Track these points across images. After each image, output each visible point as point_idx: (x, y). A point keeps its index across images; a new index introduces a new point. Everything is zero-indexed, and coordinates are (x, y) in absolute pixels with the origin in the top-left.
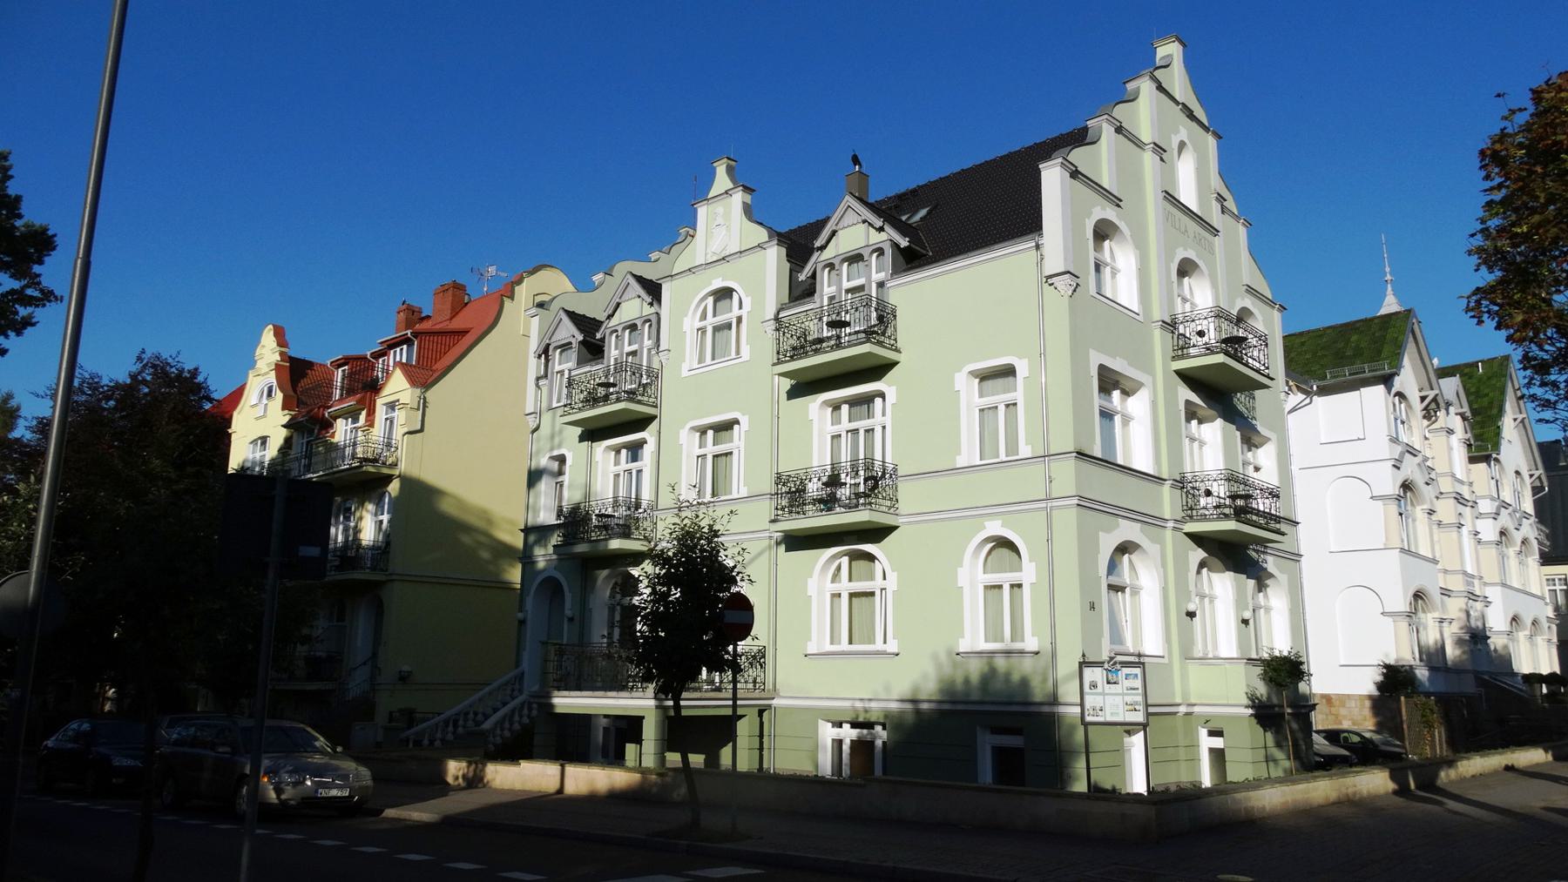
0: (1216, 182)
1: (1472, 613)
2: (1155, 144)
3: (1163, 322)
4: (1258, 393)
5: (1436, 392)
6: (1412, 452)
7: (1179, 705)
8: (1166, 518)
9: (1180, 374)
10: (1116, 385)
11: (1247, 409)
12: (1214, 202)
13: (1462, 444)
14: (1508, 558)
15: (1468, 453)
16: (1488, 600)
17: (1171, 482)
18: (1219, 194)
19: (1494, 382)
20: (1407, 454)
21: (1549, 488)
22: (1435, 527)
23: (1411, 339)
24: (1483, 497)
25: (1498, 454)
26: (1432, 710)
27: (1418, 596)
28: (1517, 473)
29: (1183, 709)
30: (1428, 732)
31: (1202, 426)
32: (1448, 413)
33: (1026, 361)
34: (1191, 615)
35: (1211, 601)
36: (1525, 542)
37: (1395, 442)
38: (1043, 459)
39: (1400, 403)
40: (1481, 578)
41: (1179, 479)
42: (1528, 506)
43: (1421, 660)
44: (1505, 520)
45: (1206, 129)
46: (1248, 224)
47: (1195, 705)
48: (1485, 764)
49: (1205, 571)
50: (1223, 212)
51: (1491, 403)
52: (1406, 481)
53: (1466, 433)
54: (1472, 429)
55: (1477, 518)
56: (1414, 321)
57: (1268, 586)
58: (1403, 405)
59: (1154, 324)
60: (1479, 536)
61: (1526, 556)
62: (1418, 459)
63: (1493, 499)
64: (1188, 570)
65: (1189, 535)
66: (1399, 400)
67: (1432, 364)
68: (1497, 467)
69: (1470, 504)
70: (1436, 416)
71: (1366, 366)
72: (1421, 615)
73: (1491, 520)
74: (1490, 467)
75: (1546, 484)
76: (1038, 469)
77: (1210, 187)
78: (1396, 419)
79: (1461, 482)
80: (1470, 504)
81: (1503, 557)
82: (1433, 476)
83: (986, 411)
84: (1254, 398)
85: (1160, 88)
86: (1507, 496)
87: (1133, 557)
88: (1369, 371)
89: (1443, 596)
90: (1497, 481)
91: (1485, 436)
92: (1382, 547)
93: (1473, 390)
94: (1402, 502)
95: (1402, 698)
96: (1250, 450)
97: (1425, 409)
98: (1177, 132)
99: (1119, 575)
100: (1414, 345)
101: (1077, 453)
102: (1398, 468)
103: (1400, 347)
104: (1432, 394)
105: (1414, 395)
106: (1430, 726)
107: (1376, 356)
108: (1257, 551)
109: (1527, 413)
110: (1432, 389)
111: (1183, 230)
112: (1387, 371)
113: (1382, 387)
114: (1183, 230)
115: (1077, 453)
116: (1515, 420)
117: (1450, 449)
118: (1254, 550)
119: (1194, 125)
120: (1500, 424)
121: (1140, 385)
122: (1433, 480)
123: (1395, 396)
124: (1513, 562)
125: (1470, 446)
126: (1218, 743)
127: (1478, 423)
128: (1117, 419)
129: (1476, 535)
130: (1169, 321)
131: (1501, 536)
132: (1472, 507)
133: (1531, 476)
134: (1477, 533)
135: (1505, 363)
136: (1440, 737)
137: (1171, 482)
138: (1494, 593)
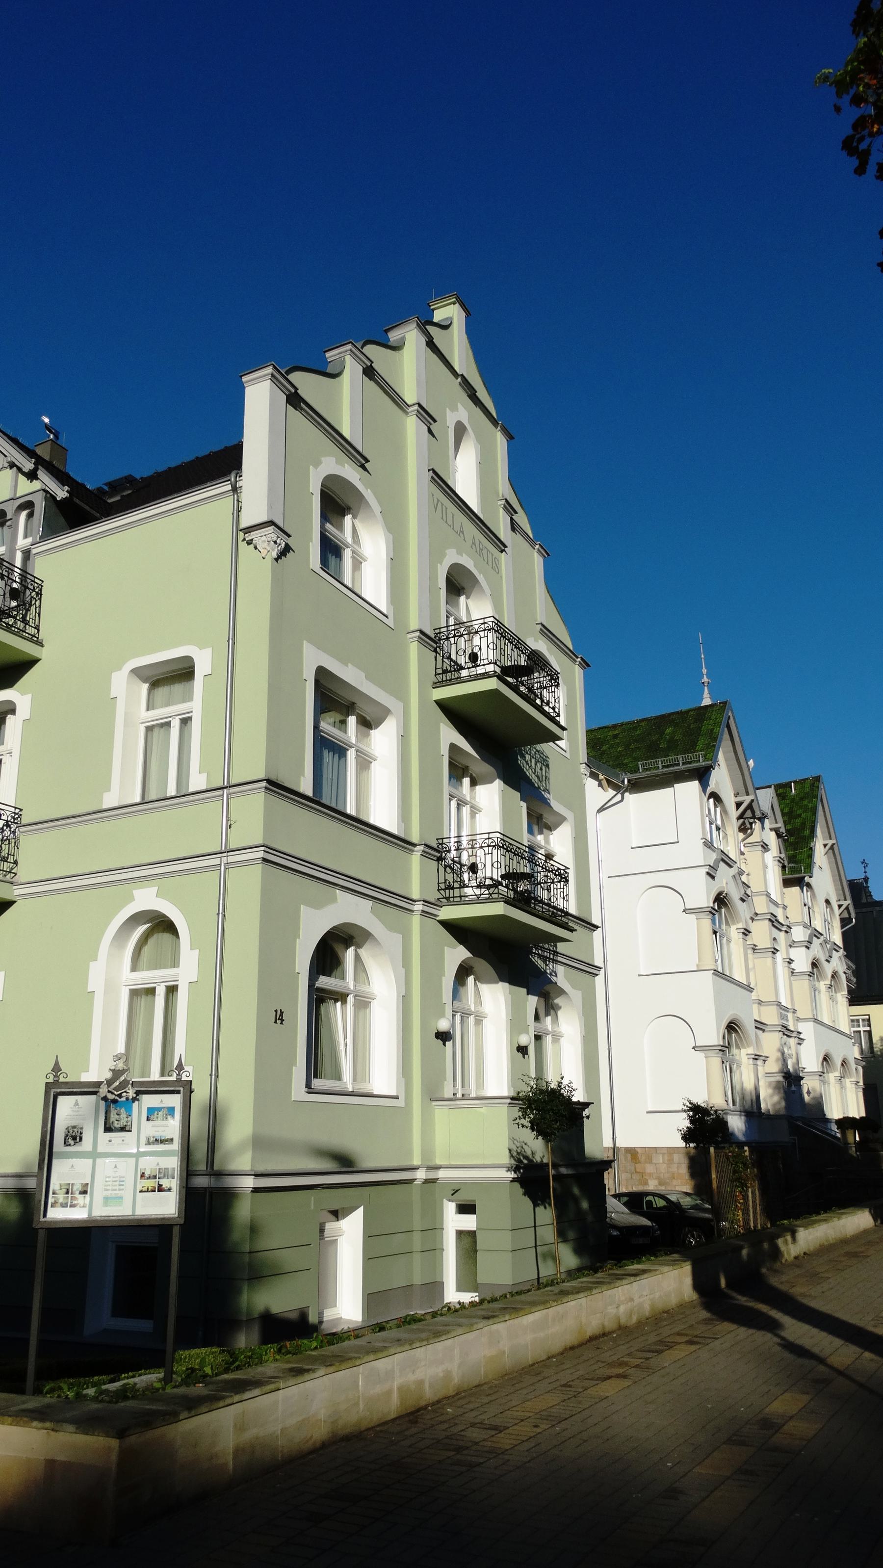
0: (504, 488)
1: (786, 1050)
2: (420, 405)
3: (422, 632)
4: (547, 748)
5: (751, 797)
6: (728, 862)
7: (414, 1169)
8: (414, 897)
9: (448, 708)
10: (348, 708)
11: (538, 776)
12: (501, 511)
13: (777, 863)
14: (819, 992)
15: (783, 875)
16: (801, 1036)
17: (422, 848)
18: (507, 501)
19: (805, 802)
20: (721, 863)
21: (855, 920)
22: (750, 952)
23: (726, 736)
24: (797, 924)
25: (811, 877)
26: (745, 1164)
27: (732, 1027)
28: (827, 902)
29: (421, 1175)
30: (740, 1192)
31: (478, 788)
32: (763, 828)
33: (209, 651)
34: (444, 1037)
35: (479, 1022)
36: (835, 975)
37: (709, 848)
38: (219, 792)
39: (716, 806)
40: (795, 1011)
41: (435, 846)
42: (837, 937)
43: (734, 1103)
44: (817, 950)
45: (495, 422)
46: (546, 553)
47: (438, 1168)
48: (811, 1237)
49: (471, 980)
50: (513, 529)
51: (804, 824)
52: (720, 894)
53: (781, 853)
54: (786, 850)
55: (790, 946)
56: (730, 714)
57: (560, 1008)
58: (718, 809)
59: (409, 636)
60: (793, 966)
61: (836, 992)
62: (733, 871)
63: (805, 926)
64: (441, 973)
65: (446, 924)
66: (715, 803)
67: (748, 766)
68: (809, 893)
69: (784, 928)
70: (751, 828)
71: (680, 757)
72: (735, 1051)
73: (804, 949)
74: (803, 892)
75: (853, 915)
76: (214, 808)
77: (498, 496)
78: (711, 823)
79: (776, 904)
80: (784, 928)
81: (815, 990)
82: (749, 892)
83: (156, 730)
84: (547, 766)
85: (431, 344)
86: (818, 924)
87: (362, 952)
88: (683, 764)
89: (757, 1030)
90: (809, 908)
91: (799, 857)
92: (696, 969)
93: (786, 810)
94: (717, 916)
95: (712, 1150)
96: (541, 833)
97: (741, 817)
98: (454, 409)
99: (343, 977)
100: (728, 737)
101: (269, 781)
102: (713, 877)
103: (715, 739)
104: (747, 800)
105: (730, 800)
106: (743, 1185)
107: (691, 747)
108: (545, 959)
109: (836, 840)
110: (748, 794)
111: (457, 528)
112: (702, 763)
113: (695, 785)
114: (457, 528)
115: (269, 781)
116: (825, 846)
117: (765, 867)
118: (539, 956)
119: (478, 411)
120: (812, 845)
121: (385, 713)
122: (749, 896)
123: (709, 798)
124: (824, 996)
125: (784, 867)
126: (469, 1222)
127: (791, 844)
128: (351, 754)
129: (789, 963)
130: (433, 636)
131: (813, 968)
132: (786, 932)
133: (840, 906)
134: (791, 961)
135: (816, 784)
136: (754, 1202)
137: (422, 848)
138: (807, 1029)
